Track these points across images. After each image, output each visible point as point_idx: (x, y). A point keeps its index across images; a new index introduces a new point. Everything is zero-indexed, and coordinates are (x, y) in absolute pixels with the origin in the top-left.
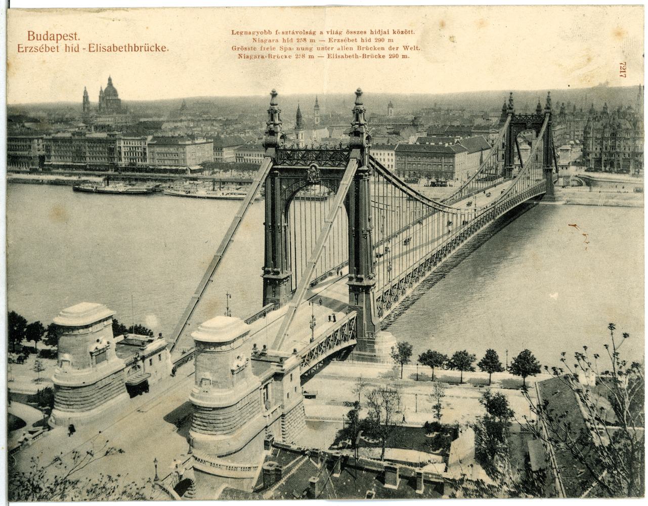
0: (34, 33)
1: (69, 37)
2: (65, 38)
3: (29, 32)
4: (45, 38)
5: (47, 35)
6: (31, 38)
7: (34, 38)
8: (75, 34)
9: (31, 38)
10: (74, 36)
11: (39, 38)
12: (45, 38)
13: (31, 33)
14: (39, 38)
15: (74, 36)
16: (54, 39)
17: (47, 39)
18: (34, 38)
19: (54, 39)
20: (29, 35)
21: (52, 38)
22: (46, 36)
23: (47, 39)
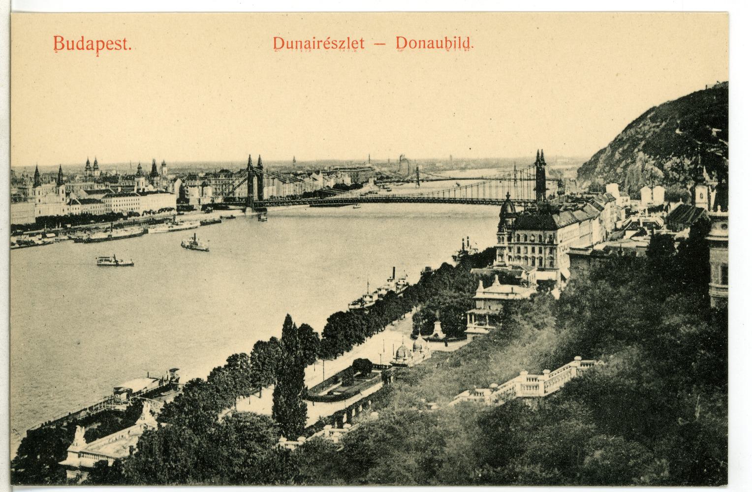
0: (62, 39)
1: (114, 46)
2: (109, 46)
3: (56, 37)
4: (80, 46)
5: (83, 41)
6: (59, 46)
7: (63, 46)
8: (125, 41)
9: (59, 46)
10: (122, 44)
11: (70, 46)
12: (80, 46)
13: (59, 39)
14: (70, 46)
15: (122, 44)
16: (92, 49)
17: (83, 49)
18: (63, 46)
19: (92, 49)
20: (56, 42)
21: (90, 47)
22: (81, 43)
23: (83, 49)
